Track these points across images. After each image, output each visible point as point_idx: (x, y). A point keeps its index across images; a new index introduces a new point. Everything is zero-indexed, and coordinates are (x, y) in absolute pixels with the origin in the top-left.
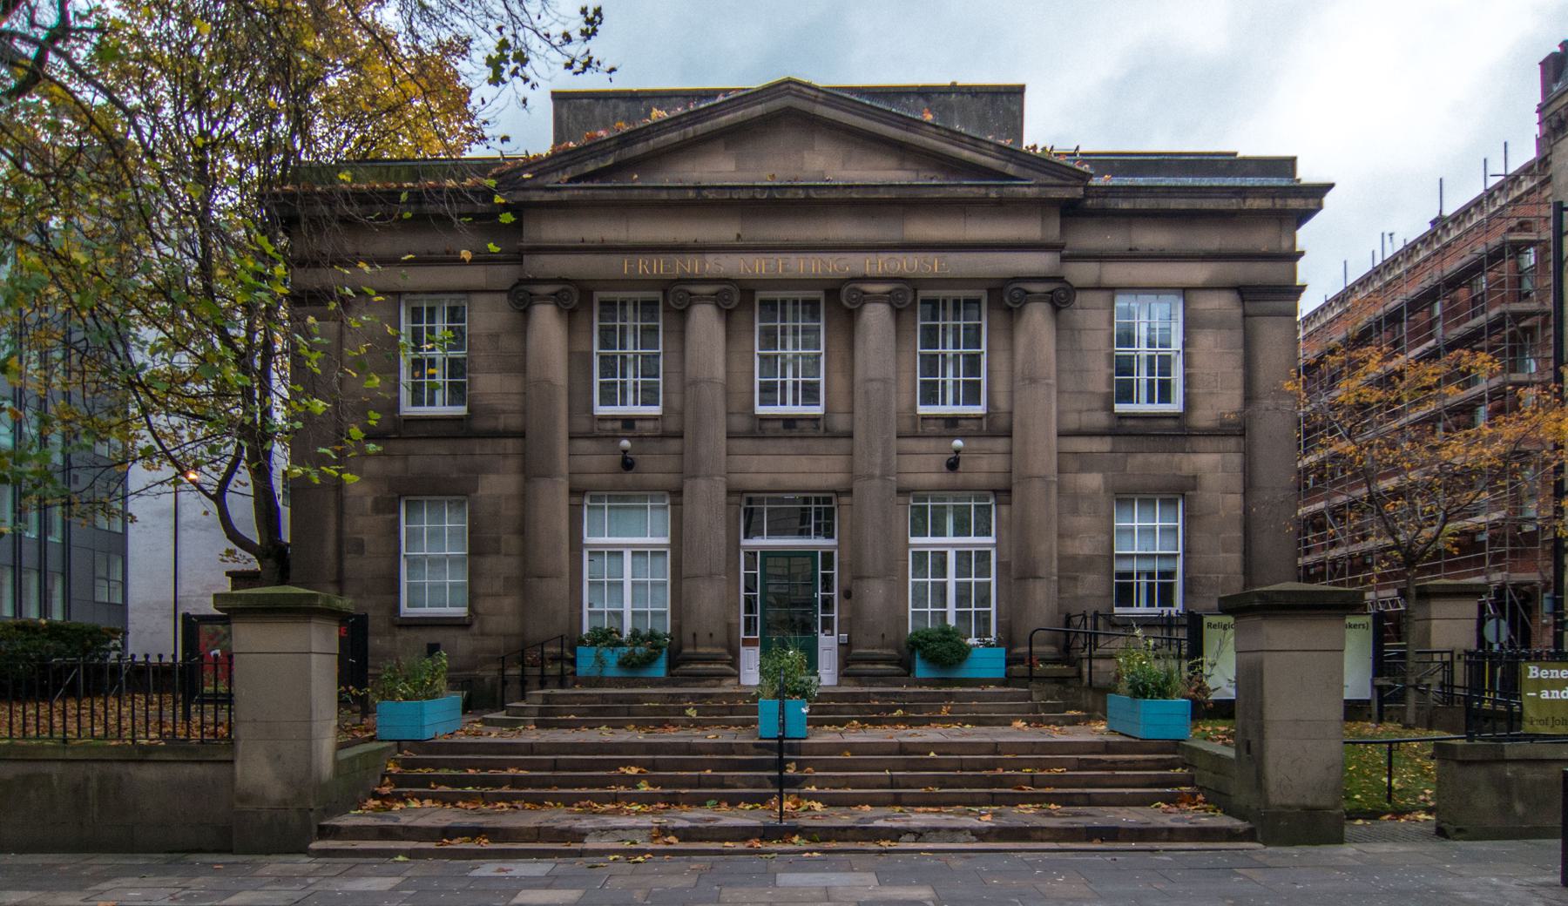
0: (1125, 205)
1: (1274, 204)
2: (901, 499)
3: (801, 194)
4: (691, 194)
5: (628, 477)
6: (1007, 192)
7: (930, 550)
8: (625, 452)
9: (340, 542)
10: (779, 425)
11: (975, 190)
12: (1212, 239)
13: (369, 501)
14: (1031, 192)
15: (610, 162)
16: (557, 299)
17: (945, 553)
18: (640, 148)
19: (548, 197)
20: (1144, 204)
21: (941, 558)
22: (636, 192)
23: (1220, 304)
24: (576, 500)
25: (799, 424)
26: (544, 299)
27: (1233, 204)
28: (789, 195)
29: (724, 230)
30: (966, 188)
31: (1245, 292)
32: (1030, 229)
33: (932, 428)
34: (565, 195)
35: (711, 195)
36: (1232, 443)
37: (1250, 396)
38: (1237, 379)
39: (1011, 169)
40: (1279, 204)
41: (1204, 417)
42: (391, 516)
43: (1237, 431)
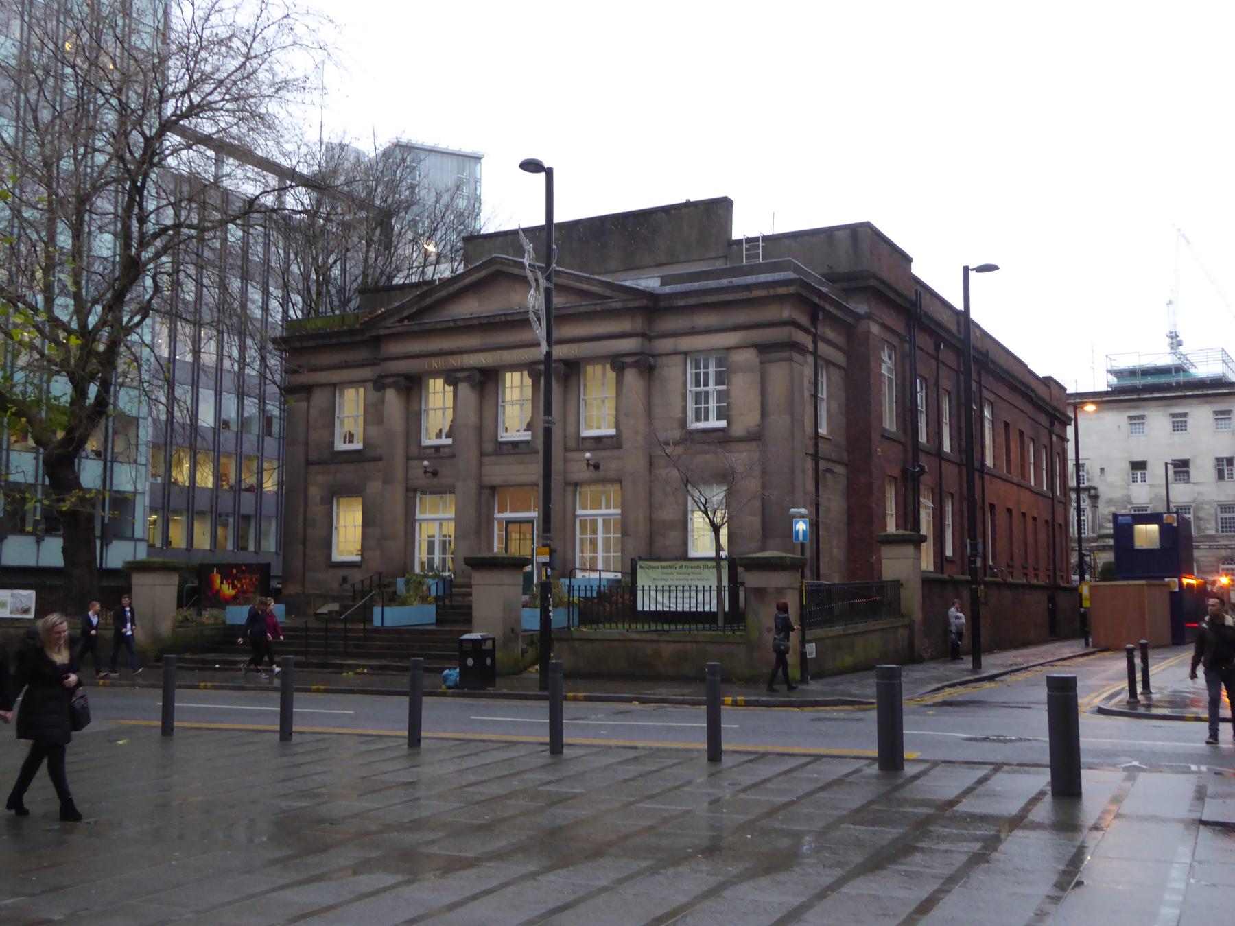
0: (681, 303)
1: (769, 292)
2: (569, 489)
3: (503, 319)
4: (452, 324)
5: (435, 481)
6: (606, 307)
7: (588, 518)
8: (425, 467)
9: (305, 520)
10: (510, 446)
11: (589, 307)
12: (741, 317)
13: (319, 498)
14: (619, 305)
15: (415, 310)
16: (395, 385)
17: (596, 520)
18: (429, 301)
19: (388, 332)
20: (692, 301)
21: (594, 522)
22: (426, 325)
23: (747, 357)
24: (410, 494)
25: (520, 445)
26: (390, 386)
27: (744, 295)
28: (497, 320)
29: (473, 341)
30: (586, 305)
31: (763, 348)
32: (625, 325)
33: (588, 444)
34: (394, 330)
35: (461, 324)
36: (754, 444)
37: (764, 414)
38: (757, 405)
39: (608, 293)
40: (772, 292)
41: (738, 430)
42: (328, 506)
43: (755, 437)
